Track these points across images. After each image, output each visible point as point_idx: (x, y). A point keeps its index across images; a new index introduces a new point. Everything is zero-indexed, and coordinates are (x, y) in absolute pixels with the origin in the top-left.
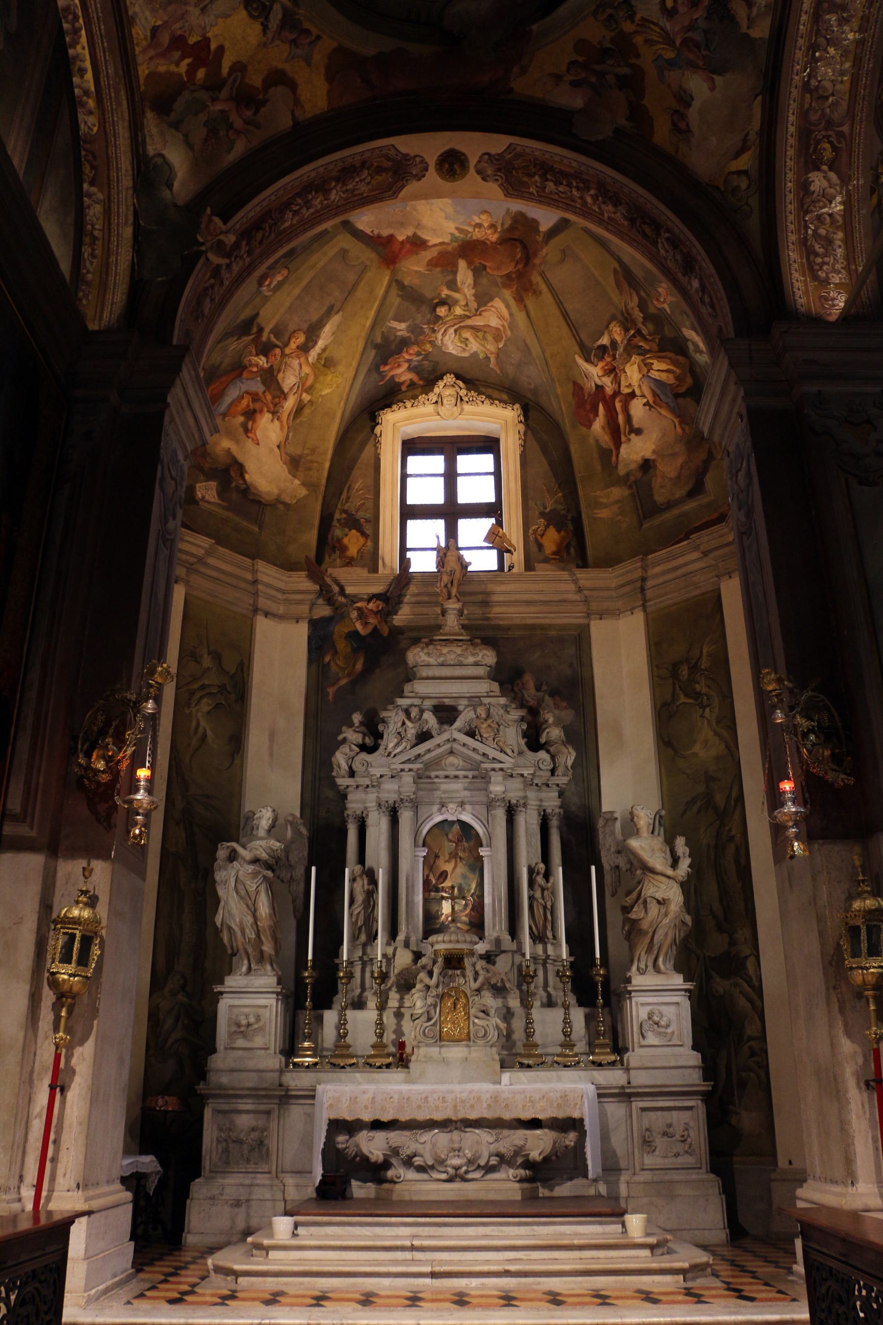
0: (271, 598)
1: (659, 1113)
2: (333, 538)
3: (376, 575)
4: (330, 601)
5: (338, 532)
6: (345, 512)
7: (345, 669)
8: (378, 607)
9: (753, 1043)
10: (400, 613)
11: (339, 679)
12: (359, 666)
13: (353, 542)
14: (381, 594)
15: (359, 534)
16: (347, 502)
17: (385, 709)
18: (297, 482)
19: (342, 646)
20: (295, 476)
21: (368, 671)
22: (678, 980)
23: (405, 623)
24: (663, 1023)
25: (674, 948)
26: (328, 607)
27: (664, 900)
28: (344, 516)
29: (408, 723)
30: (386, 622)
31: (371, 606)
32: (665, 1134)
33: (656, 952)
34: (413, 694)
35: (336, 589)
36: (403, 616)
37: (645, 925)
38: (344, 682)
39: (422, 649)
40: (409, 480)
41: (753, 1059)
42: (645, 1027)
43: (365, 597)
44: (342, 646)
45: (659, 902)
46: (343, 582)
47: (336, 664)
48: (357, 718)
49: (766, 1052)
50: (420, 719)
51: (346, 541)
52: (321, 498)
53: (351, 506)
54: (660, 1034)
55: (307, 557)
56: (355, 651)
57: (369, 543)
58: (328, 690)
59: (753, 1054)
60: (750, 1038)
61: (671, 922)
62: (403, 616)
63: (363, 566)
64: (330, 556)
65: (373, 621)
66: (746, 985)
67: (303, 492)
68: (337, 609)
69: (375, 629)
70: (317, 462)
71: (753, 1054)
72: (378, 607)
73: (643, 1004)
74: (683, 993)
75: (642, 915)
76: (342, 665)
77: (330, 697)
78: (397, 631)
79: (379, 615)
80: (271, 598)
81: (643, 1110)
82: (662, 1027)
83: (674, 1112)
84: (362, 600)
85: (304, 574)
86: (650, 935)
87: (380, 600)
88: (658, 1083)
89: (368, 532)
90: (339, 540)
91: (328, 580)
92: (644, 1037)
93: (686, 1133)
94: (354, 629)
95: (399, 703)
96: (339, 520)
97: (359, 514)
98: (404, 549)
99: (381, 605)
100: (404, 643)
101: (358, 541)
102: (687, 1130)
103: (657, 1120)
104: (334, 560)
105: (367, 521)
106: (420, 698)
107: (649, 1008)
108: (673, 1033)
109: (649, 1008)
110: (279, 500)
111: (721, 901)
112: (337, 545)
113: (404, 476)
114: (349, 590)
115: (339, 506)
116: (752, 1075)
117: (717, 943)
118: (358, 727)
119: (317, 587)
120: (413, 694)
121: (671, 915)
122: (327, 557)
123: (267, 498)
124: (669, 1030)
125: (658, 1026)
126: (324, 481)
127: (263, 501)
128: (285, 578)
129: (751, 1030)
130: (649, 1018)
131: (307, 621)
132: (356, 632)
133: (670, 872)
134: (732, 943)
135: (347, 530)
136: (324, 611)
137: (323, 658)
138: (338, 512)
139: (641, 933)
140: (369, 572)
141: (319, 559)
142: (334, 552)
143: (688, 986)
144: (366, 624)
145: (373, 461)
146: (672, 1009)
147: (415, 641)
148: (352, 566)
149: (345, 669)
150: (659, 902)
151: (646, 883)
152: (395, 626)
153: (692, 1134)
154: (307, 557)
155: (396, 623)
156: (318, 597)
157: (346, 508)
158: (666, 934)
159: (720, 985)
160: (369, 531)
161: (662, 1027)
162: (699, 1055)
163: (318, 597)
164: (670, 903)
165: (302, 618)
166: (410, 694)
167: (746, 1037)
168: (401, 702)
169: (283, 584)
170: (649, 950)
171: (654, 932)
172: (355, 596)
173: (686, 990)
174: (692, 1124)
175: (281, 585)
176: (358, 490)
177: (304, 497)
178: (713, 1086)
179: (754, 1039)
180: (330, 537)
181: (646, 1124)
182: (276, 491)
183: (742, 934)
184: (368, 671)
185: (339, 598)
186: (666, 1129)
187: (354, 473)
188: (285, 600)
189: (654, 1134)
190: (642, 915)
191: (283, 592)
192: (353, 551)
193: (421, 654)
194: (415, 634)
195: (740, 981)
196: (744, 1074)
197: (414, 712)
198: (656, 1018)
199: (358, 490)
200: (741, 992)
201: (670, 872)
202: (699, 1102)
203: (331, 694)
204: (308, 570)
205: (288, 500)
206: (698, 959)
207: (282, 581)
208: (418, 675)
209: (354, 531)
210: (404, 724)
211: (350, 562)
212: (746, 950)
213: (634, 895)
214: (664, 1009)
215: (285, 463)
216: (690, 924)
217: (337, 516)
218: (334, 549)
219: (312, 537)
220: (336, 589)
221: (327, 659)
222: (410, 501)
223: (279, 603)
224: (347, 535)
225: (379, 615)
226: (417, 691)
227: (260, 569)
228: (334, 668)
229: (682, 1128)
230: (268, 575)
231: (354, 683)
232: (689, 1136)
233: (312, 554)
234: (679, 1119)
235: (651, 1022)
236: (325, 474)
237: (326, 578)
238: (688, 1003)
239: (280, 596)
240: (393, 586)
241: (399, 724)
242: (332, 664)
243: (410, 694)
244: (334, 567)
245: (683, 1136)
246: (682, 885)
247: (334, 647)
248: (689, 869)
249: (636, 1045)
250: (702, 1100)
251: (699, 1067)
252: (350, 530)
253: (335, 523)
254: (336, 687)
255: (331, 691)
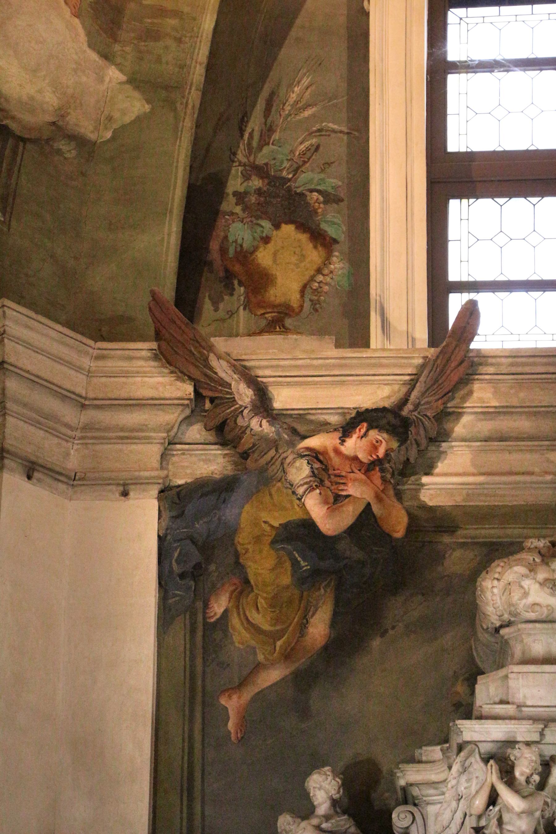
0: (45, 421)
2: (223, 251)
3: (365, 353)
4: (224, 433)
5: (239, 232)
6: (261, 171)
7: (274, 637)
8: (375, 448)
10: (440, 467)
11: (258, 667)
12: (319, 628)
13: (287, 261)
14: (384, 409)
15: (304, 237)
16: (264, 142)
17: (413, 760)
18: (114, 74)
19: (264, 566)
20: (107, 57)
21: (344, 646)
23: (459, 500)
26: (216, 451)
28: (256, 183)
29: (507, 796)
30: (399, 496)
31: (354, 445)
34: (510, 709)
35: (244, 394)
36: (452, 477)
38: (273, 675)
39: (532, 568)
40: (453, 80)
43: (334, 419)
44: (264, 566)
46: (264, 374)
47: (247, 622)
48: (323, 788)
50: (541, 786)
51: (264, 257)
52: (188, 124)
53: (278, 154)
55: (153, 294)
56: (307, 581)
57: (338, 265)
58: (223, 701)
62: (452, 477)
63: (320, 332)
64: (215, 304)
65: (359, 490)
67: (135, 106)
68: (245, 455)
69: (367, 515)
70: (177, 14)
72: (375, 448)
76: (266, 627)
77: (231, 725)
78: (432, 525)
79: (377, 475)
80: (45, 421)
84: (323, 427)
85: (145, 347)
87: (381, 428)
89: (331, 231)
90: (245, 256)
91: (222, 369)
94: (295, 515)
95: (467, 736)
96: (240, 197)
97: (303, 177)
98: (439, 286)
99: (383, 442)
100: (456, 561)
101: (303, 257)
104: (231, 314)
105: (330, 198)
106: (535, 719)
110: (59, 129)
112: (237, 268)
113: (439, 70)
114: (283, 398)
115: (241, 156)
118: (327, 818)
119: (188, 389)
120: (510, 709)
122: (208, 306)
123: (27, 118)
126: (198, 74)
127: (13, 126)
128: (86, 362)
131: (154, 491)
132: (308, 525)
135: (266, 224)
136: (206, 462)
137: (206, 605)
138: (236, 171)
140: (338, 345)
141: (187, 300)
142: (231, 291)
144: (337, 500)
145: (342, 20)
147: (497, 551)
148: (286, 331)
149: (274, 637)
152: (424, 507)
154: (153, 294)
155: (429, 497)
156: (188, 420)
157: (261, 159)
160: (333, 223)
163: (188, 420)
165: (140, 482)
166: (500, 709)
168: (470, 730)
169: (82, 378)
172: (302, 416)
175: (77, 383)
176: (299, 108)
177: (139, 119)
180: (214, 245)
182: (51, 99)
184: (344, 646)
185: (254, 423)
187: (283, 53)
188: (85, 428)
191: (82, 403)
192: (287, 286)
193: (526, 583)
194: (489, 532)
197: (525, 766)
199: (299, 108)
203: (232, 713)
204: (158, 337)
205: (87, 128)
207: (79, 369)
208: (517, 651)
209: (288, 229)
210: (493, 799)
211: (278, 320)
215: (77, 15)
217: (235, 183)
218: (228, 279)
219: (163, 241)
220: (244, 394)
221: (219, 605)
222: (455, 143)
223: (67, 439)
224: (266, 240)
225: (377, 475)
226: (519, 697)
227: (13, 329)
228: (239, 634)
230: (38, 351)
231: (304, 680)
233: (168, 292)
236: (203, 52)
237: (214, 362)
239: (68, 414)
240: (419, 388)
241: (480, 802)
242: (235, 621)
243: (500, 709)
244: (232, 334)
247: (238, 566)
252: (277, 226)
253: (229, 204)
254: (248, 694)
255: (233, 704)
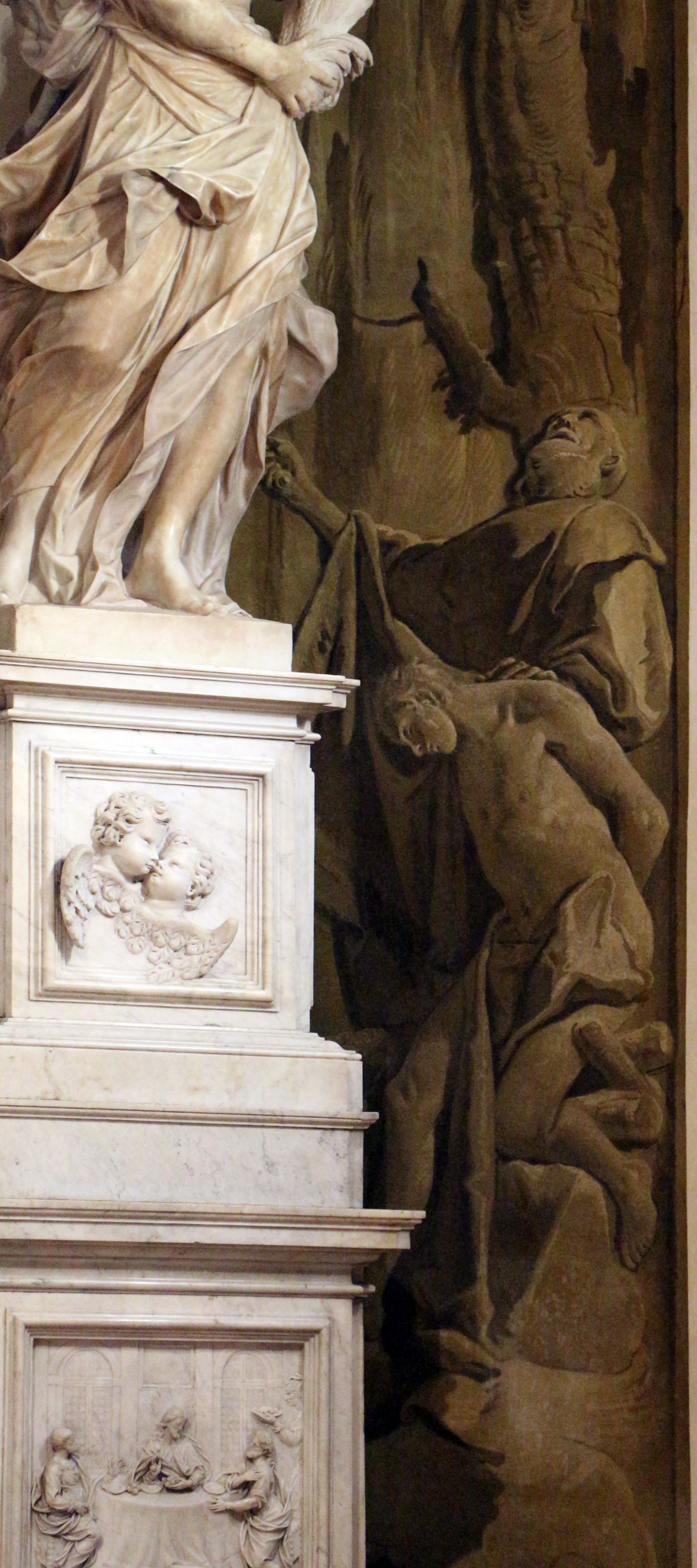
1: (129, 1355)
9: (592, 1017)
22: (263, 653)
24: (172, 877)
25: (240, 475)
27: (216, 202)
32: (150, 1472)
33: (145, 488)
37: (103, 330)
41: (591, 1100)
42: (77, 890)
45: (189, 211)
49: (672, 1071)
54: (152, 933)
59: (594, 1074)
60: (585, 994)
61: (242, 332)
66: (585, 715)
71: (594, 1074)
73: (68, 766)
74: (288, 725)
75: (91, 269)
81: (44, 1336)
82: (169, 897)
83: (203, 1357)
86: (121, 391)
88: (135, 1196)
92: (65, 940)
93: (262, 1467)
102: (267, 1454)
103: (114, 1395)
107: (98, 792)
108: (226, 932)
109: (98, 792)
111: (484, 251)
116: (585, 1183)
117: (441, 479)
121: (249, 298)
124: (205, 919)
125: (147, 894)
129: (599, 946)
130: (102, 845)
133: (256, 47)
134: (528, 485)
139: (74, 366)
143: (328, 691)
146: (230, 802)
150: (189, 211)
151: (118, 91)
153: (291, 1478)
158: (213, 397)
159: (442, 703)
161: (169, 897)
162: (352, 1064)
164: (248, 229)
167: (562, 985)
170: (112, 469)
171: (150, 376)
173: (302, 712)
174: (293, 1424)
178: (418, 1233)
179: (612, 997)
181: (48, 1415)
183: (594, 443)
186: (157, 1447)
189: (96, 1474)
190: (91, 269)
195: (555, 689)
196: (535, 1172)
198: (138, 851)
200: (552, 749)
201: (256, 47)
202: (343, 1310)
206: (325, 550)
212: (604, 532)
213: (41, 152)
214: (186, 802)
216: (329, 358)
229: (239, 1445)
232: (274, 1485)
234: (231, 1393)
235: (109, 866)
238: (305, 782)
245: (247, 1486)
246: (306, 127)
248: (363, 50)
249: (19, 985)
250: (356, 1300)
251: (351, 1127)
